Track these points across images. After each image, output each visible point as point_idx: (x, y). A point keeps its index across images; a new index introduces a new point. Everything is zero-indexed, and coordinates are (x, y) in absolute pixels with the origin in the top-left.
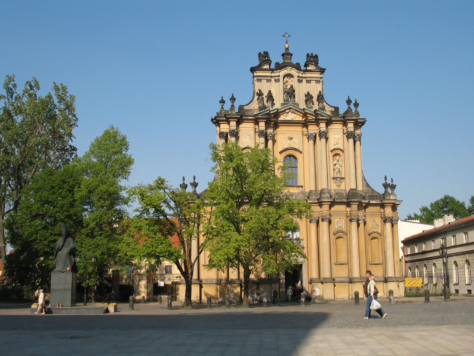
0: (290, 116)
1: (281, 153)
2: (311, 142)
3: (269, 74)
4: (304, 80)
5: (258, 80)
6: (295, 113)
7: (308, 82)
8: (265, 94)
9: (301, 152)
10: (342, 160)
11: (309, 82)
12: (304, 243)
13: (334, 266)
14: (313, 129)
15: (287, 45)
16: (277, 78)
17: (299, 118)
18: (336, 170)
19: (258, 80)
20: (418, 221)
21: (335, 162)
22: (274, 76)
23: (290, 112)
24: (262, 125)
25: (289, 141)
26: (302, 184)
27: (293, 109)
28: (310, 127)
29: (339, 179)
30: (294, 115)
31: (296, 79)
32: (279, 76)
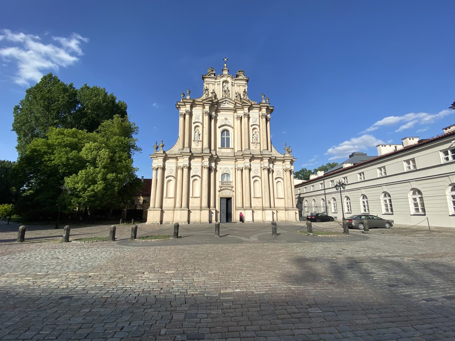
0: (227, 106)
2: (239, 121)
3: (214, 80)
4: (236, 85)
6: (229, 104)
8: (211, 91)
13: (252, 199)
14: (240, 113)
15: (225, 64)
16: (218, 83)
17: (232, 106)
18: (254, 138)
21: (254, 133)
22: (217, 82)
23: (226, 104)
26: (233, 147)
28: (238, 112)
30: (228, 105)
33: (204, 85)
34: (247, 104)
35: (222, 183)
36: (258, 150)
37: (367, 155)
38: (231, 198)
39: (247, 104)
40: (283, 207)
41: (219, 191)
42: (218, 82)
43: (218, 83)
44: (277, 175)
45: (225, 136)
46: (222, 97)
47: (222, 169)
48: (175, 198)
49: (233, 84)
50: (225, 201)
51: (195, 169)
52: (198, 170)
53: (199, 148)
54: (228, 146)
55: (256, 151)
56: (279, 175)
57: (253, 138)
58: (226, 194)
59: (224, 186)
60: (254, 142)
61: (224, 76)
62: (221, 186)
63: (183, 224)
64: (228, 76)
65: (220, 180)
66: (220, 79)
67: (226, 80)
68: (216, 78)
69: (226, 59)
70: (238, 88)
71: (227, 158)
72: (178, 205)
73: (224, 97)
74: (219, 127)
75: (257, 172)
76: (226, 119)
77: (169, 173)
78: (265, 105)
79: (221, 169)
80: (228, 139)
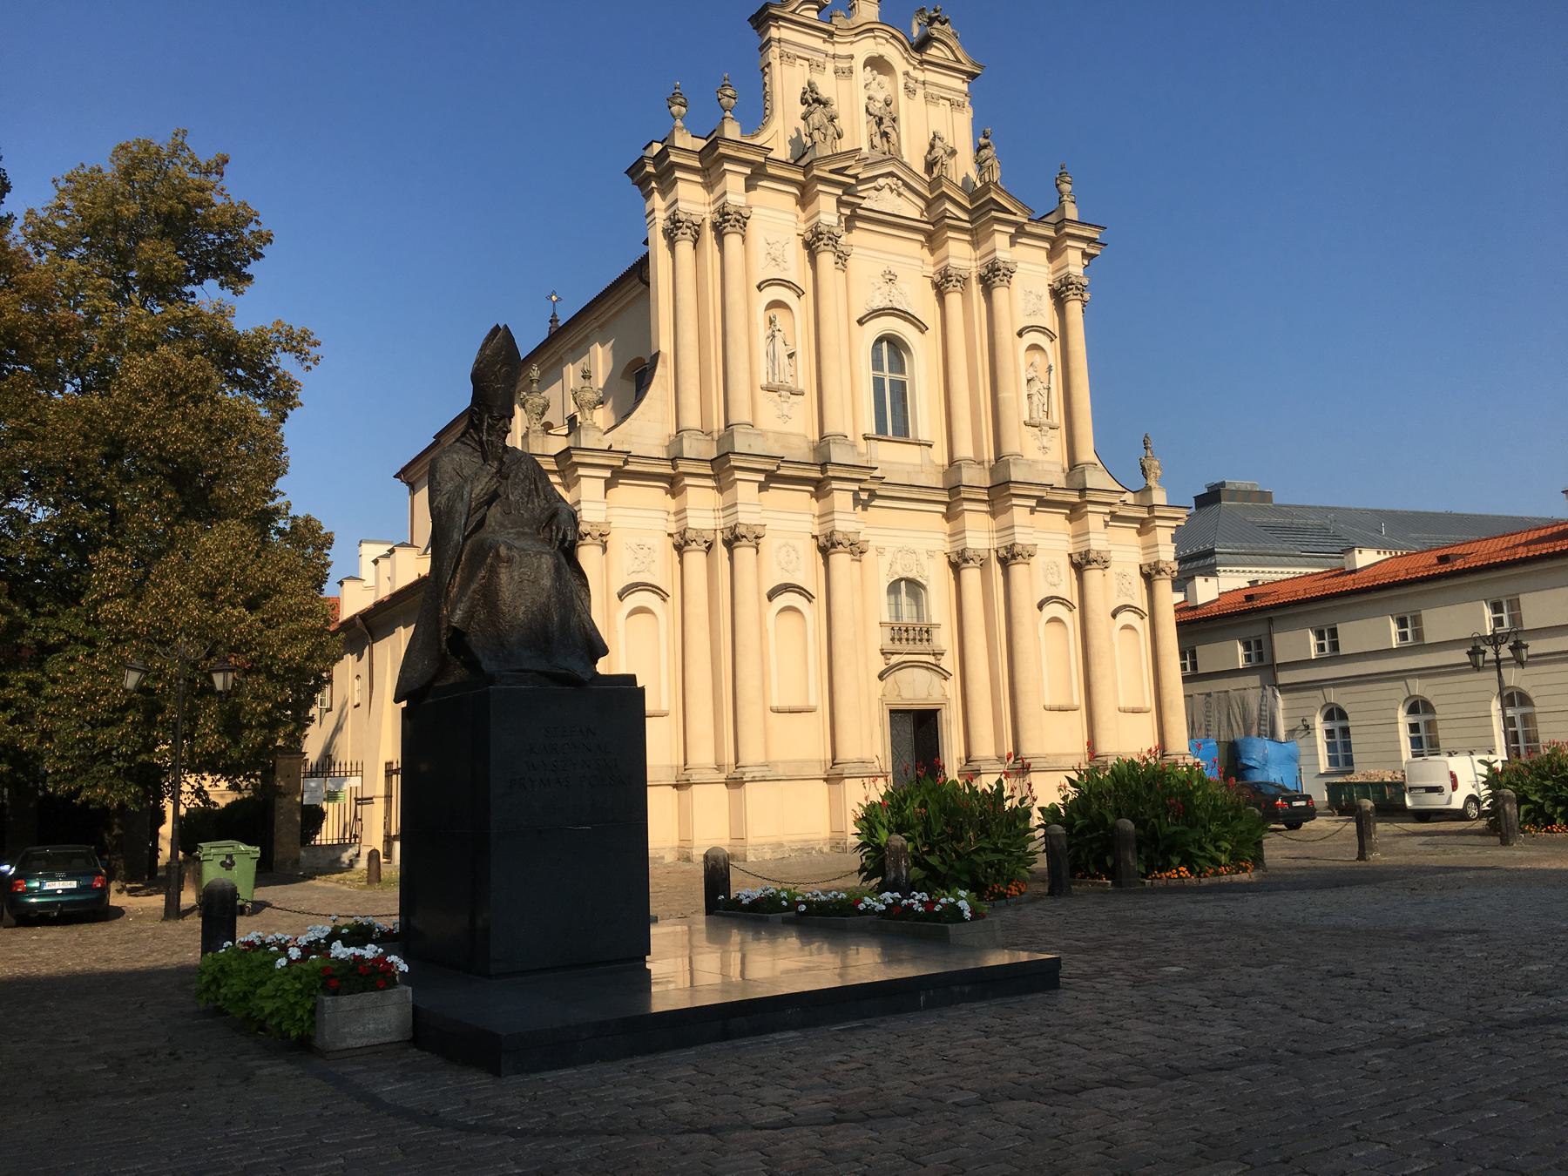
1: (860, 322)
4: (920, 92)
5: (785, 58)
6: (900, 194)
7: (929, 99)
9: (922, 328)
10: (1050, 367)
11: (930, 99)
12: (945, 638)
14: (961, 254)
16: (843, 64)
18: (1035, 399)
19: (785, 58)
22: (834, 57)
23: (886, 191)
24: (827, 209)
25: (886, 288)
27: (899, 178)
29: (1047, 428)
31: (901, 80)
32: (852, 57)
33: (771, 60)
34: (1012, 217)
35: (893, 629)
36: (1054, 463)
37: (1275, 501)
39: (1012, 217)
41: (881, 677)
42: (840, 57)
43: (843, 64)
45: (887, 375)
47: (888, 558)
49: (911, 84)
50: (908, 728)
51: (784, 550)
53: (795, 431)
55: (1046, 467)
56: (1126, 595)
57: (1030, 396)
58: (917, 689)
59: (904, 646)
60: (1036, 421)
61: (872, 30)
62: (889, 647)
63: (768, 857)
64: (894, 37)
66: (852, 43)
67: (881, 57)
68: (831, 34)
70: (931, 108)
71: (909, 494)
74: (860, 322)
75: (1055, 580)
76: (891, 278)
77: (635, 568)
78: (1085, 234)
79: (880, 551)
80: (900, 390)
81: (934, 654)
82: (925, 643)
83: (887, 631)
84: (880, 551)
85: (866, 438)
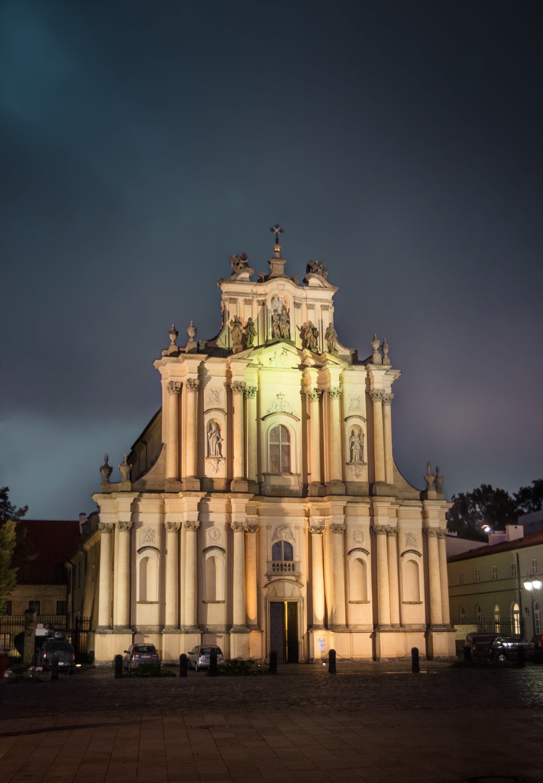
10: (363, 434)
11: (310, 307)
18: (354, 451)
20: (456, 534)
35: (274, 565)
38: (297, 603)
40: (419, 624)
41: (266, 586)
44: (406, 546)
46: (270, 338)
48: (162, 602)
52: (220, 534)
54: (287, 470)
56: (411, 545)
65: (270, 559)
69: (277, 230)
70: (310, 312)
72: (170, 621)
73: (277, 339)
75: (360, 539)
81: (294, 576)
82: (291, 571)
83: (271, 565)
84: (268, 527)
85: (264, 474)
